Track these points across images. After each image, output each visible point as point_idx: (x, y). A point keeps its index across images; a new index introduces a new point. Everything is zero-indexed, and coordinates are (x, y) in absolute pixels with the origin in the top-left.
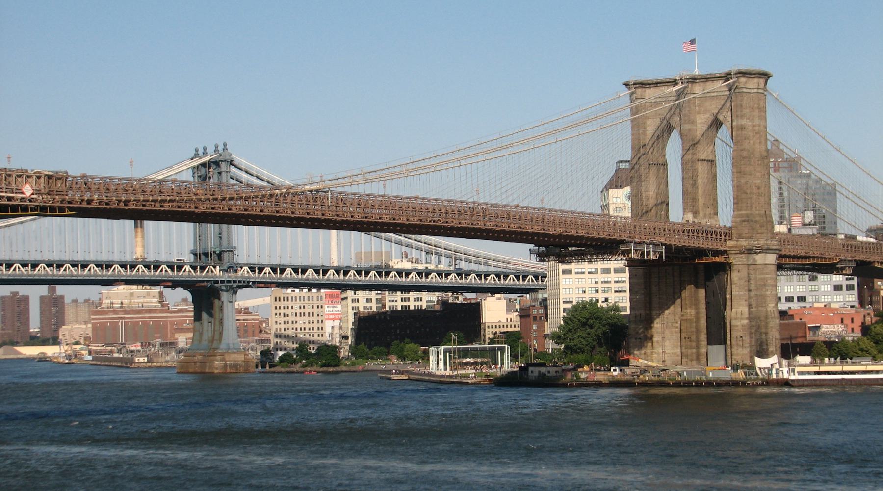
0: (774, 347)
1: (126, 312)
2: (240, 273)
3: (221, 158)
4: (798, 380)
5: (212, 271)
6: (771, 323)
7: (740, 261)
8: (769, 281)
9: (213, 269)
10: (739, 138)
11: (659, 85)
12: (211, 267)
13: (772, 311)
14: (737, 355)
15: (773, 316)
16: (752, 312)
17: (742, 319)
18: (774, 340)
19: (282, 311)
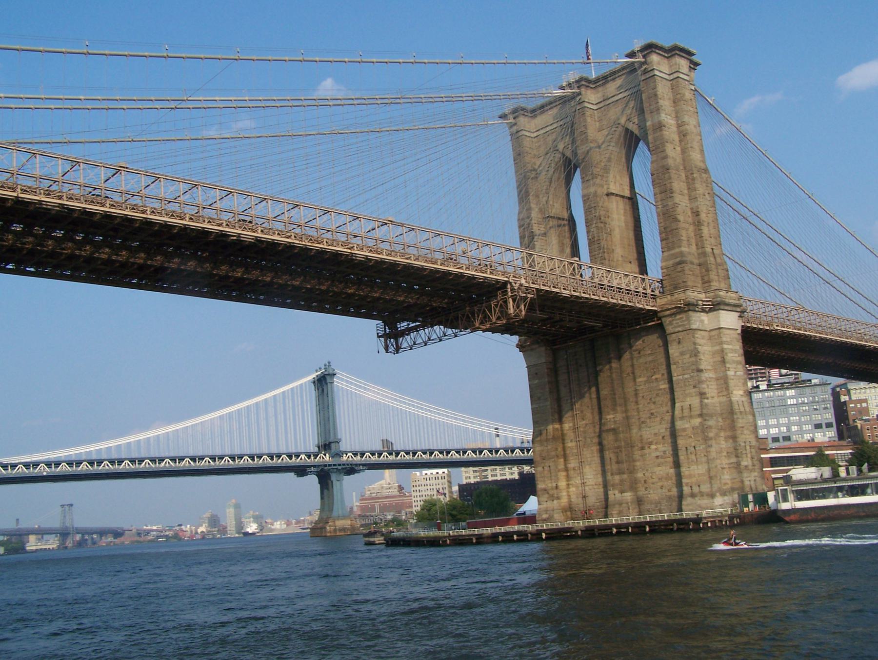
0: (749, 459)
1: (379, 498)
2: (345, 458)
3: (326, 373)
4: (794, 511)
5: (323, 458)
6: (740, 421)
7: (679, 326)
8: (730, 355)
9: (324, 457)
10: (658, 143)
11: (546, 108)
12: (322, 455)
13: (740, 403)
14: (690, 476)
15: (742, 409)
16: (706, 405)
17: (691, 417)
18: (748, 447)
19: (418, 488)
